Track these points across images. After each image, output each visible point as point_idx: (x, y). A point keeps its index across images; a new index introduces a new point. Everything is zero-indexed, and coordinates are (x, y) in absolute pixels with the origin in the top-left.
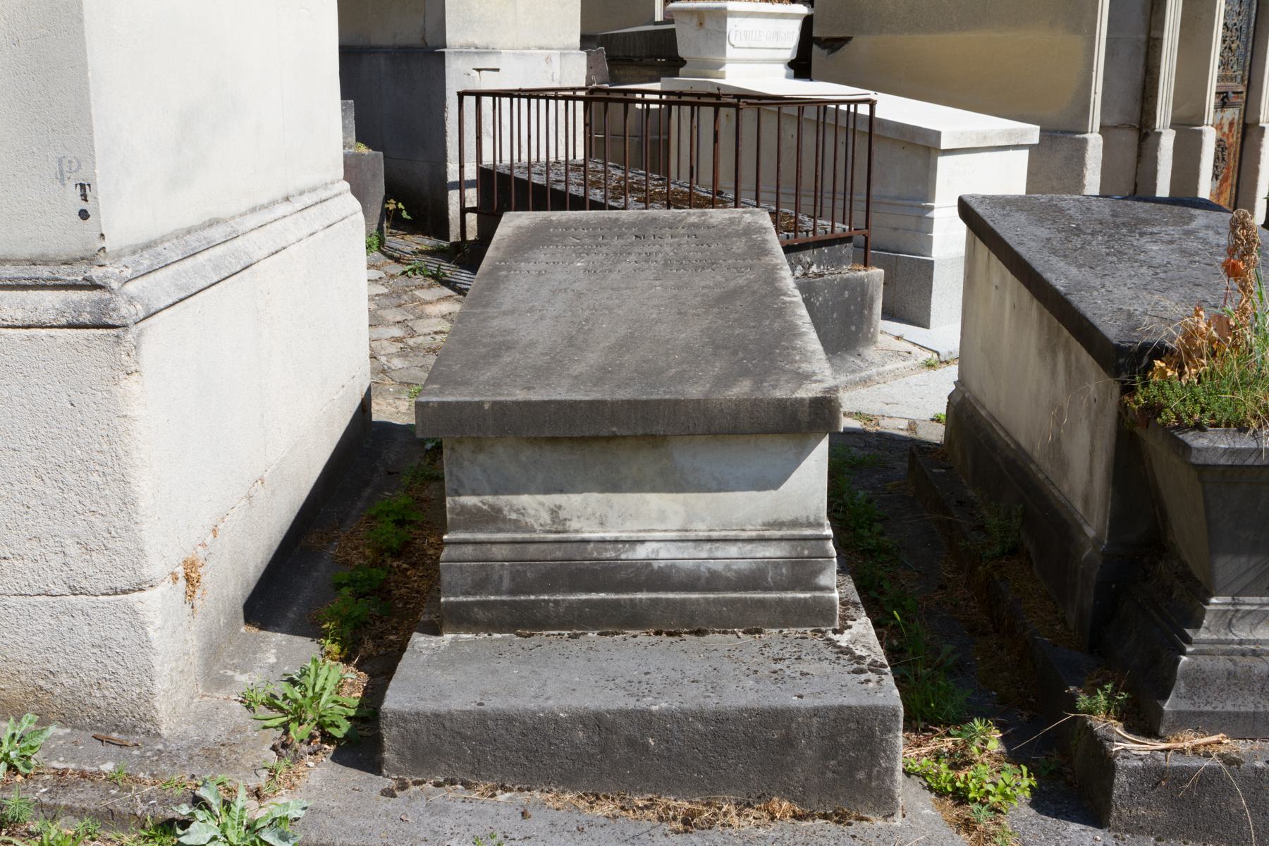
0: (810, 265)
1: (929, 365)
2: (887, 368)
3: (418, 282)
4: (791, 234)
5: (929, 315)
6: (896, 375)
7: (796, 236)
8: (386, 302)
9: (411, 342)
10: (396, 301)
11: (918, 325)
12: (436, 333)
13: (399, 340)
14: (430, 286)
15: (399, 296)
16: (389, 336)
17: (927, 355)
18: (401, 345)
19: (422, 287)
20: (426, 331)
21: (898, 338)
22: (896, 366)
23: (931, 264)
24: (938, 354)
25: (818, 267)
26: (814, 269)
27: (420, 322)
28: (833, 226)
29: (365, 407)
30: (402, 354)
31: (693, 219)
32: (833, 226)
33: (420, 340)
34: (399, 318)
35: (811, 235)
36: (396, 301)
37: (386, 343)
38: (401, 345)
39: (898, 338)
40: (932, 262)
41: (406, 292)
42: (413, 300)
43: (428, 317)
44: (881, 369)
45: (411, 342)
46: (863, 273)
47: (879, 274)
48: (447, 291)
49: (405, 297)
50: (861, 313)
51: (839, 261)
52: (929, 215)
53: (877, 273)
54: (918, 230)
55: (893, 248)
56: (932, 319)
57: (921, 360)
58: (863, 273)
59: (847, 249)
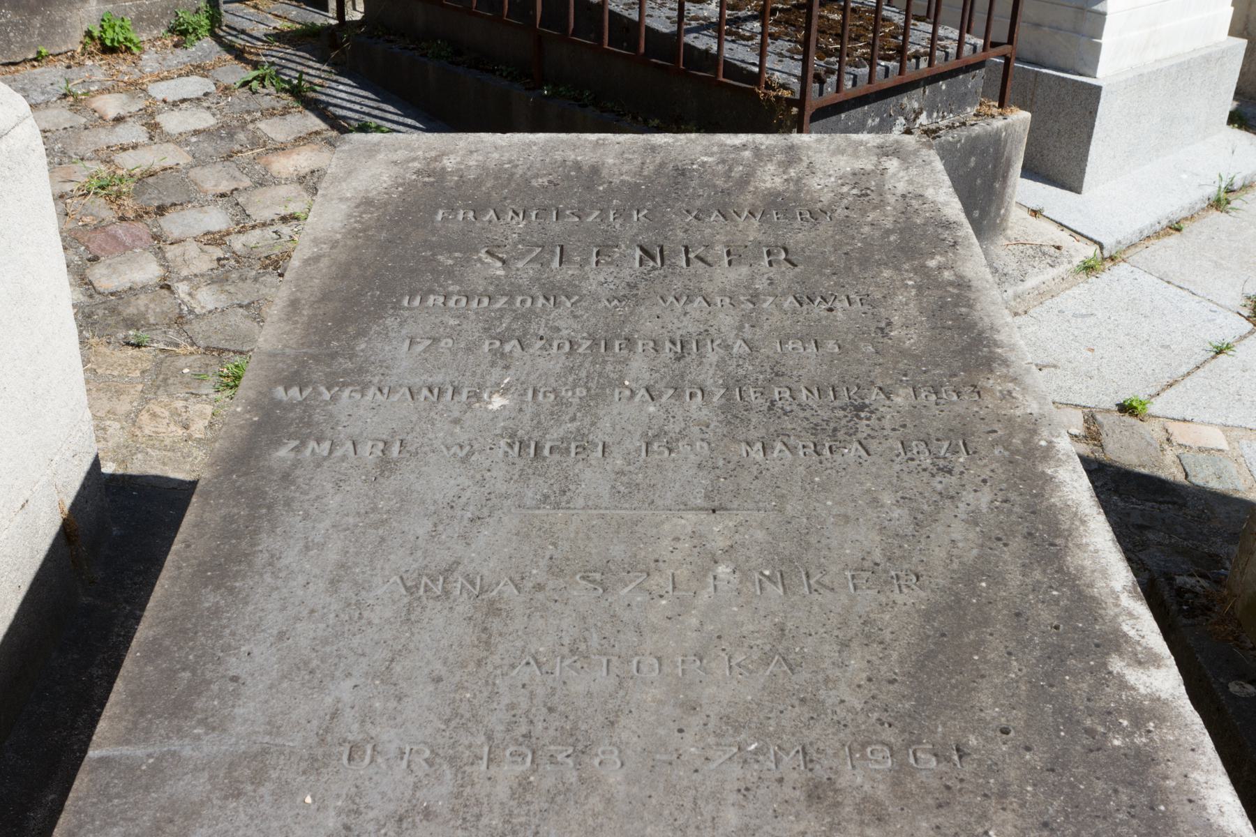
0: (918, 114)
1: (1088, 268)
2: (1031, 282)
3: (267, 102)
4: (893, 65)
5: (1083, 172)
6: (1043, 295)
7: (901, 71)
8: (207, 147)
9: (238, 243)
10: (224, 147)
11: (1063, 186)
12: (284, 219)
13: (216, 239)
14: (286, 111)
15: (231, 135)
16: (198, 230)
17: (1090, 251)
18: (218, 252)
19: (270, 113)
20: (267, 215)
21: (1035, 213)
22: (1041, 278)
23: (1094, 93)
24: (1101, 247)
25: (930, 116)
26: (923, 119)
27: (260, 196)
28: (961, 42)
29: (96, 464)
30: (218, 278)
31: (770, 178)
32: (961, 42)
33: (253, 237)
34: (225, 187)
35: (923, 64)
36: (224, 147)
37: (192, 249)
38: (218, 252)
39: (1035, 213)
40: (1097, 90)
41: (243, 126)
42: (255, 142)
43: (276, 182)
44: (1021, 288)
45: (238, 243)
46: (998, 123)
47: (1023, 121)
48: (314, 122)
49: (241, 136)
50: (991, 187)
51: (960, 102)
52: (1098, 7)
53: (1020, 118)
54: (1076, 31)
55: (1033, 58)
56: (1088, 178)
57: (1077, 261)
58: (998, 123)
59: (975, 81)
